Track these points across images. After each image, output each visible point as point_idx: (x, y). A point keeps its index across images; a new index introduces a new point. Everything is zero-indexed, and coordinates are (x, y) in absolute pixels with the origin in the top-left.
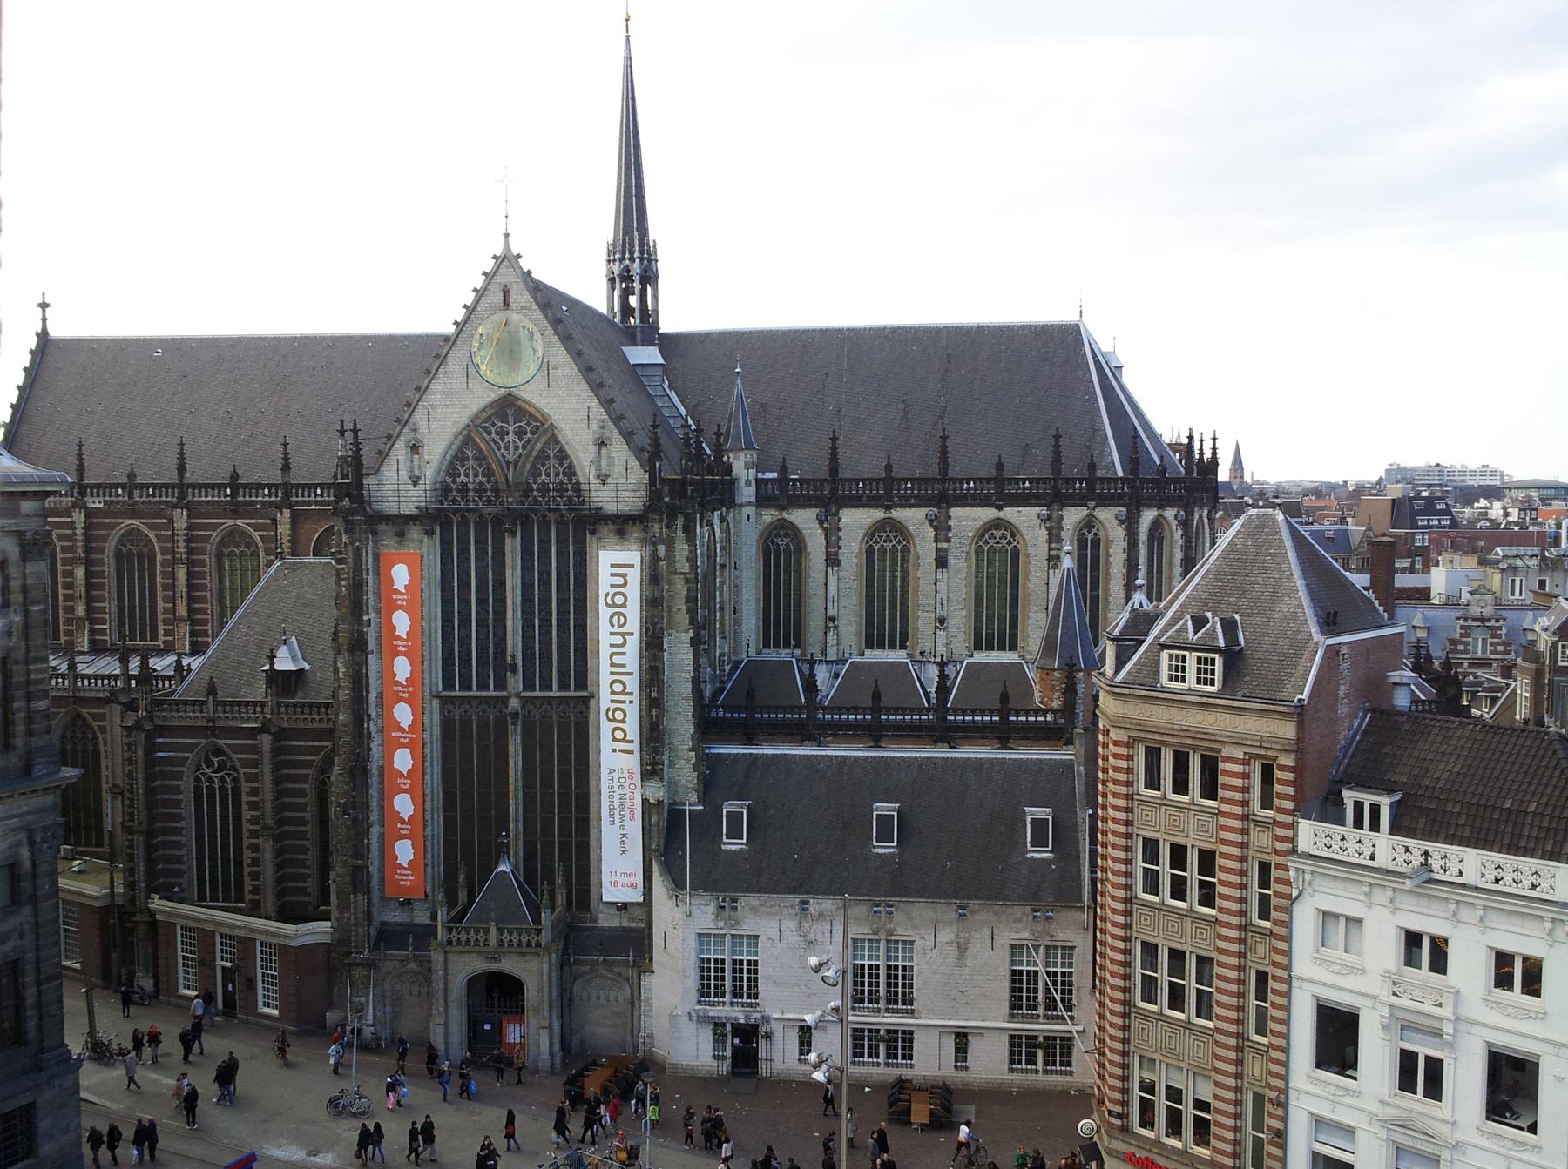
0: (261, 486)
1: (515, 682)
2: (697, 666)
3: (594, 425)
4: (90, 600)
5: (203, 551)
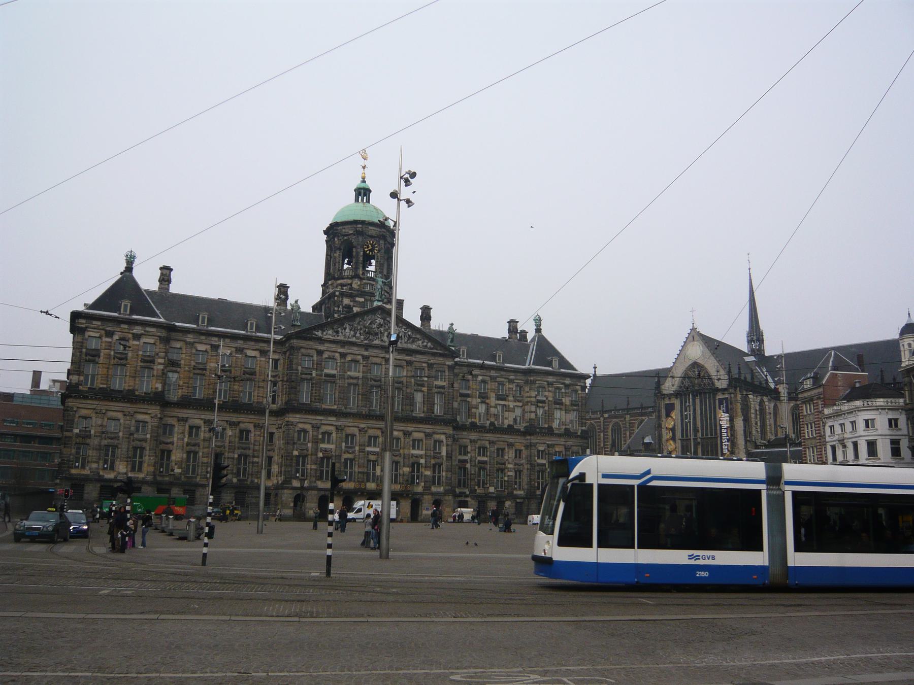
0: (649, 407)
1: (699, 435)
2: (745, 427)
3: (716, 367)
4: (604, 442)
5: (634, 426)
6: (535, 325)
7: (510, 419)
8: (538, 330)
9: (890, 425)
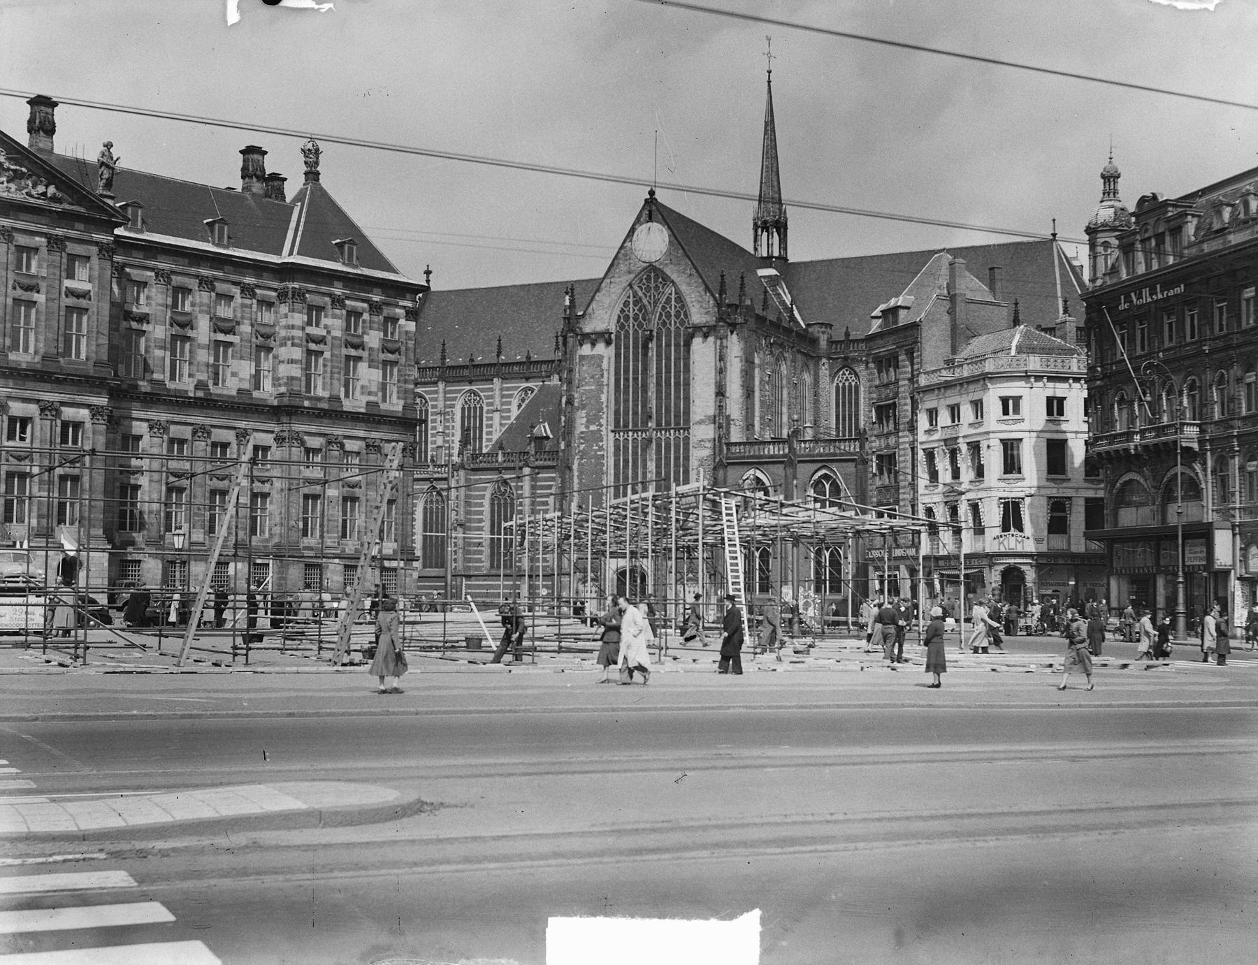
6: (306, 163)
7: (241, 376)
8: (312, 175)
9: (1050, 412)
